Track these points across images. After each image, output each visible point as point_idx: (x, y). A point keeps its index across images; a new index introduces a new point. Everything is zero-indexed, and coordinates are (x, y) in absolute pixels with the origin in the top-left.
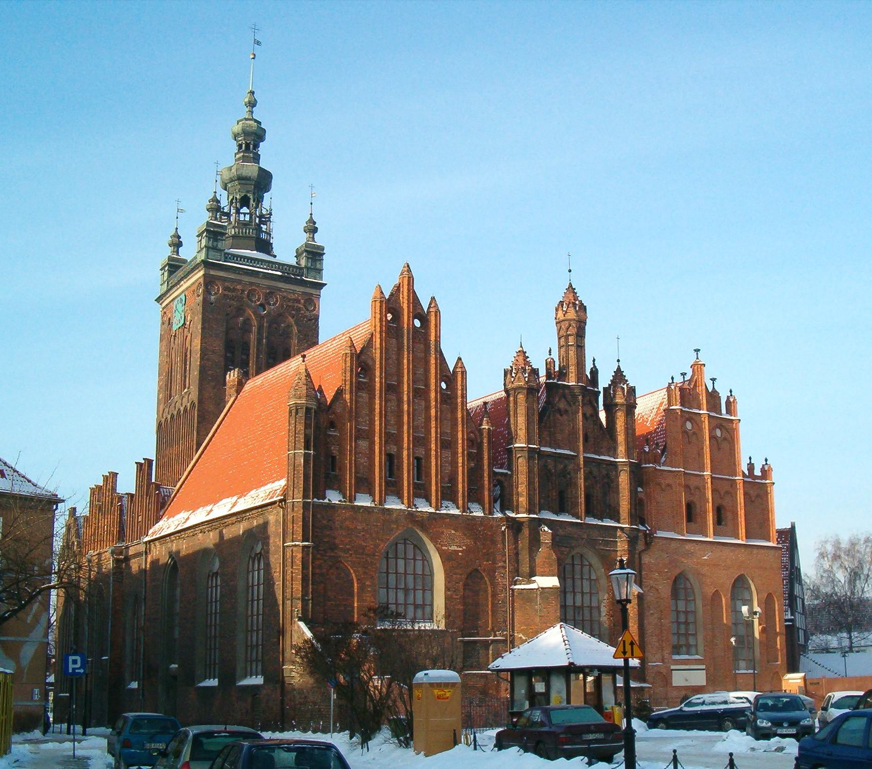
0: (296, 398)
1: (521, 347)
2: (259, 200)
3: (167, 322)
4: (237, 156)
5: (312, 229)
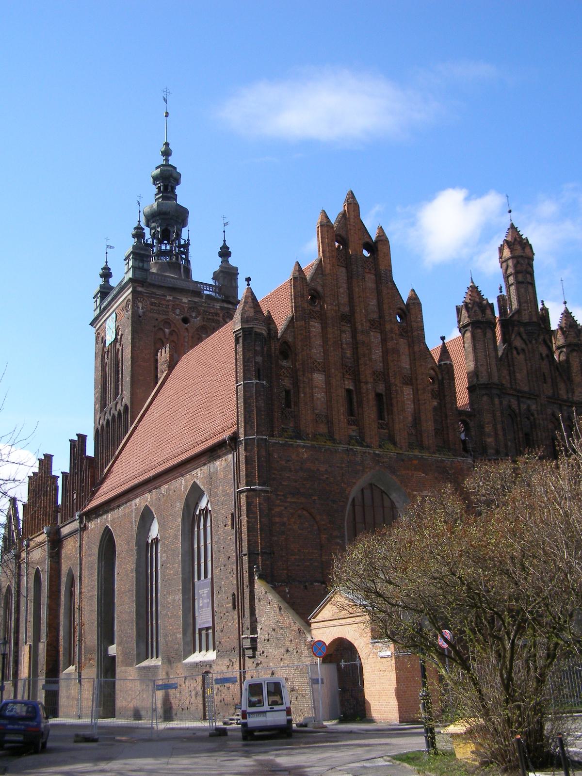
1: (472, 282)
3: (100, 339)
4: (157, 197)
5: (225, 253)
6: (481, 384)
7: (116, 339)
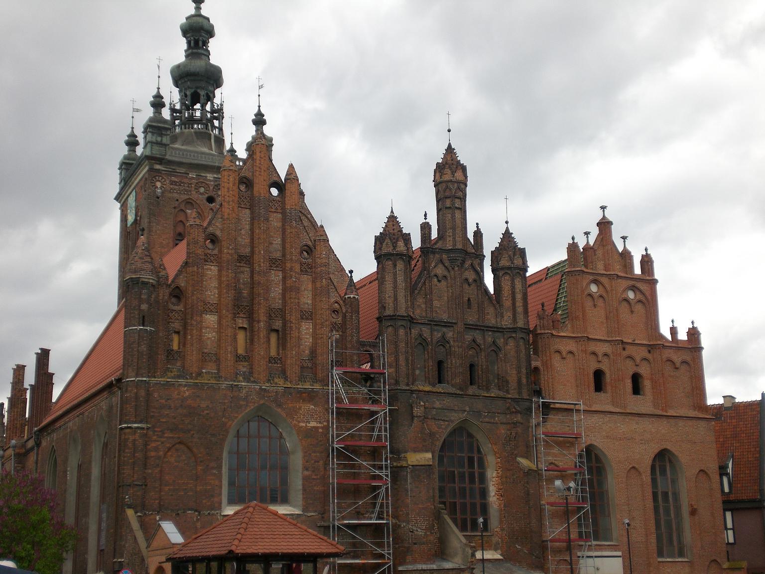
0: (132, 272)
2: (210, 98)
5: (259, 121)
6: (386, 316)
7: (136, 220)
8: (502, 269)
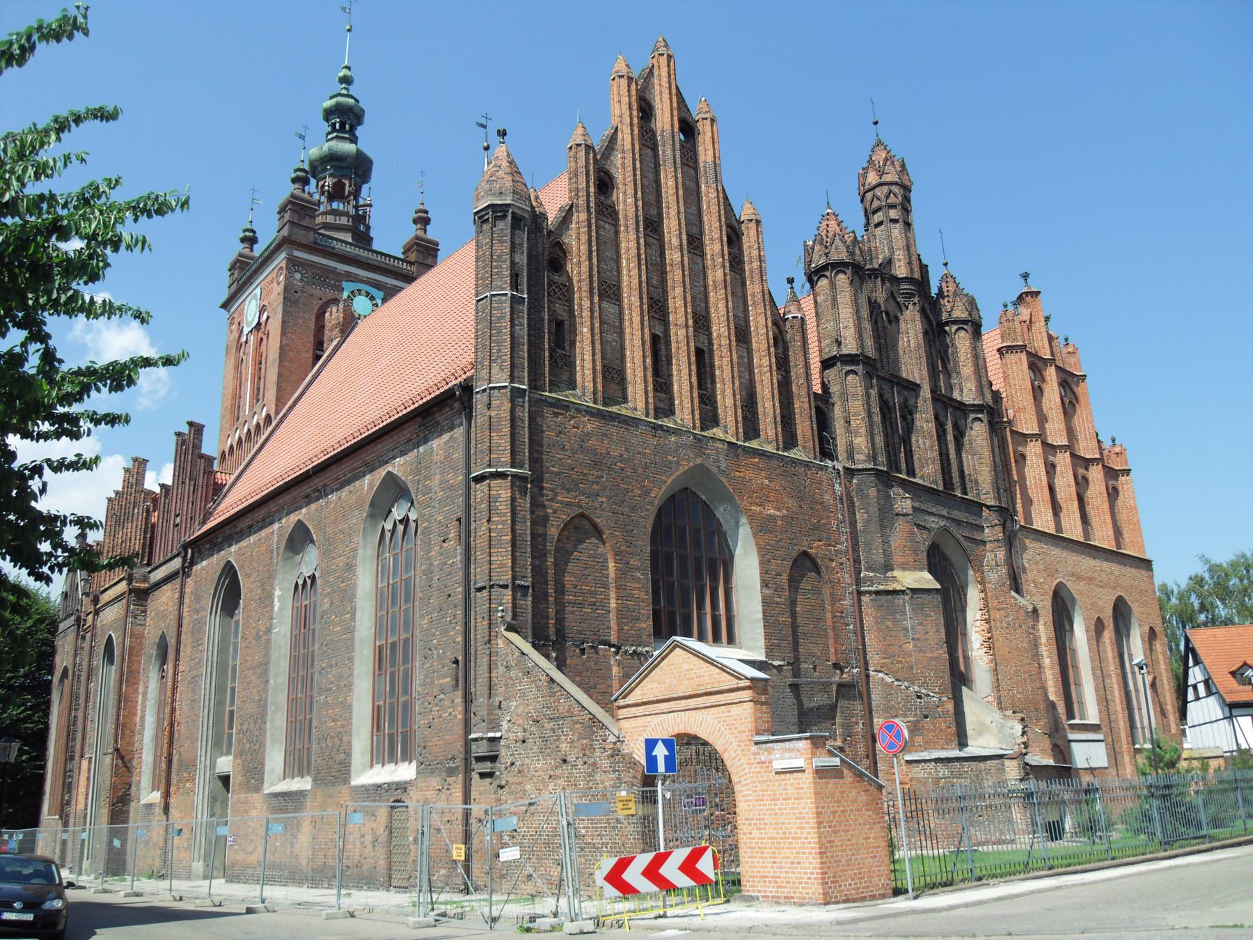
4: (330, 137)
5: (423, 220)
7: (259, 324)
8: (955, 322)
